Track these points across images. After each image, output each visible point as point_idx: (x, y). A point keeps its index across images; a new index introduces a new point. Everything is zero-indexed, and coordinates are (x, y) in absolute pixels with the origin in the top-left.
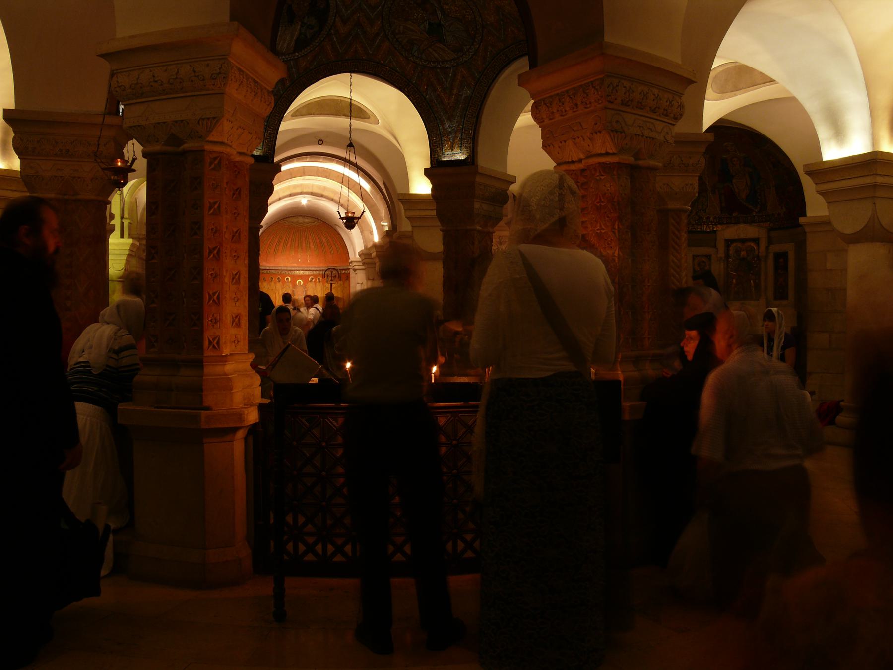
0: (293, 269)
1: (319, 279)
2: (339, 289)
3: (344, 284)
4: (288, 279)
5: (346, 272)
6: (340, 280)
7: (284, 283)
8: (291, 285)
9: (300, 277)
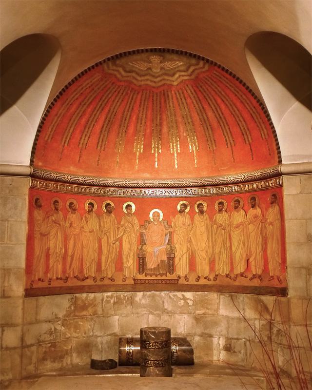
0: (141, 183)
1: (200, 205)
2: (251, 227)
4: (128, 206)
5: (271, 183)
6: (253, 206)
7: (120, 215)
8: (136, 221)
9: (157, 202)
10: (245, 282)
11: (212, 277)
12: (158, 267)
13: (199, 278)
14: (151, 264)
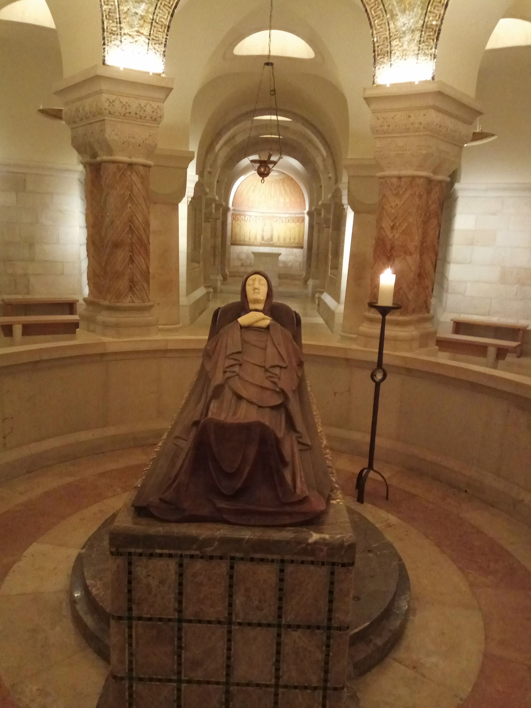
3: (300, 224)
10: (293, 245)
11: (284, 243)
12: (268, 239)
13: (280, 244)
14: (266, 238)
